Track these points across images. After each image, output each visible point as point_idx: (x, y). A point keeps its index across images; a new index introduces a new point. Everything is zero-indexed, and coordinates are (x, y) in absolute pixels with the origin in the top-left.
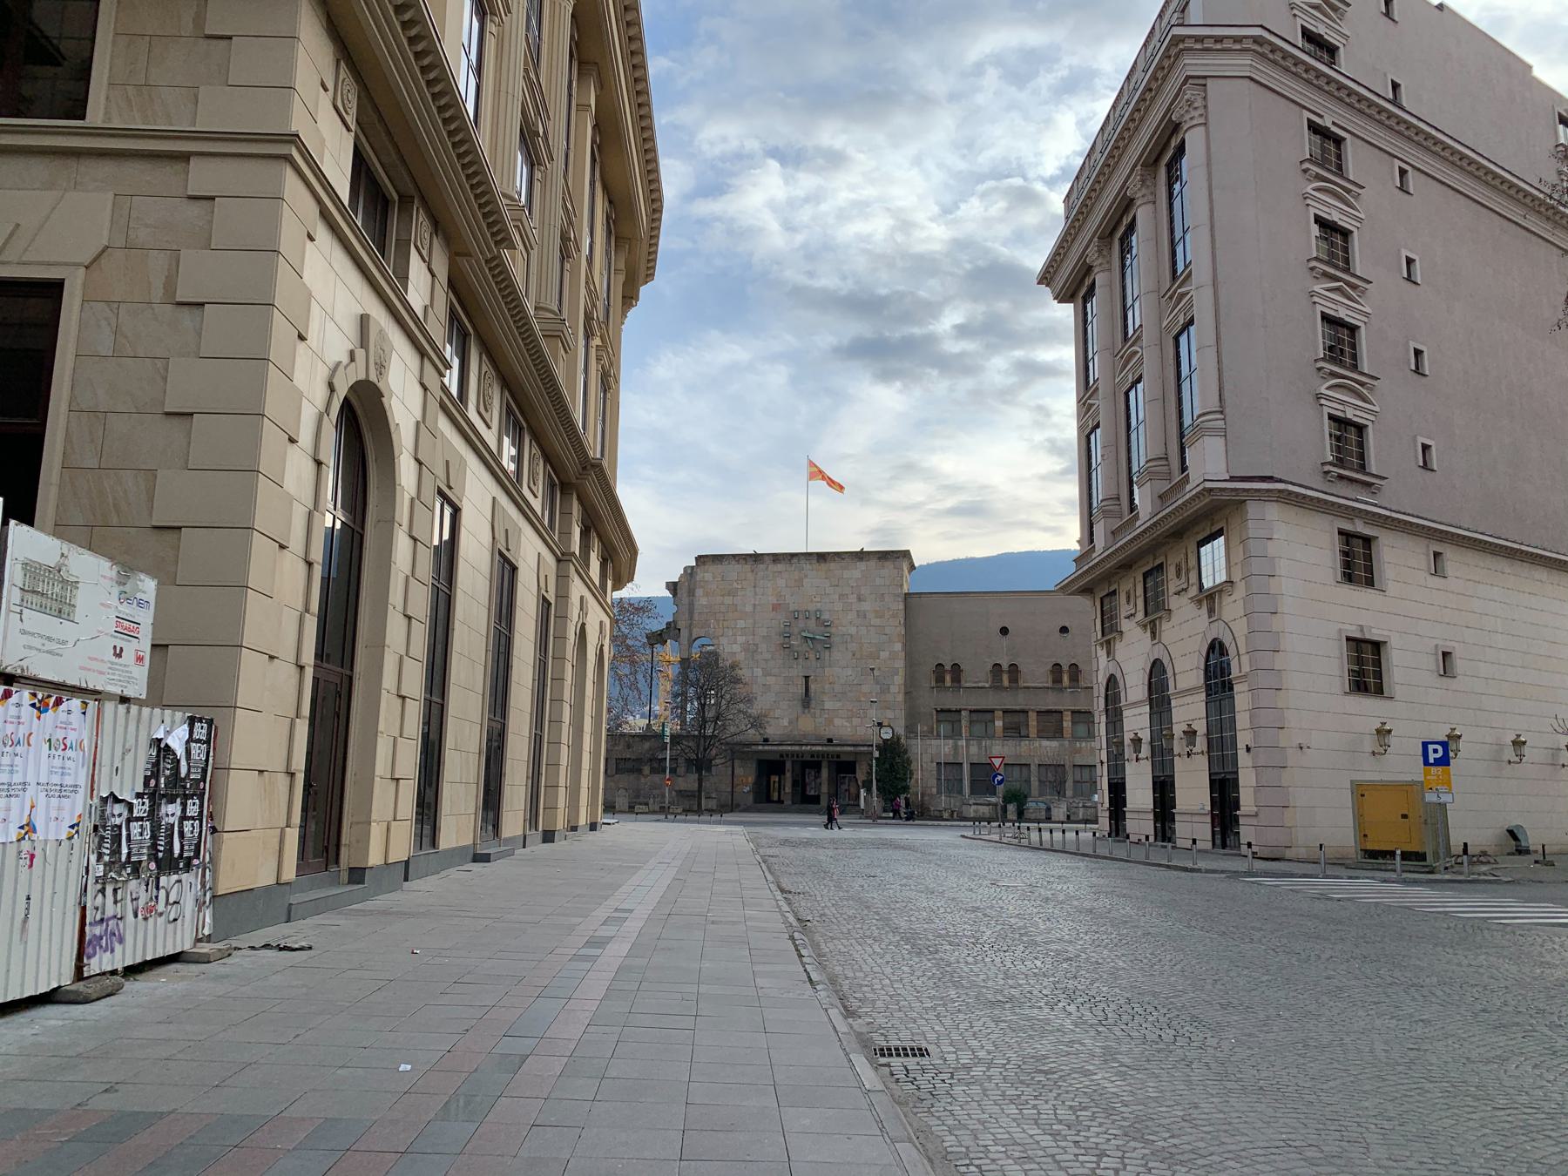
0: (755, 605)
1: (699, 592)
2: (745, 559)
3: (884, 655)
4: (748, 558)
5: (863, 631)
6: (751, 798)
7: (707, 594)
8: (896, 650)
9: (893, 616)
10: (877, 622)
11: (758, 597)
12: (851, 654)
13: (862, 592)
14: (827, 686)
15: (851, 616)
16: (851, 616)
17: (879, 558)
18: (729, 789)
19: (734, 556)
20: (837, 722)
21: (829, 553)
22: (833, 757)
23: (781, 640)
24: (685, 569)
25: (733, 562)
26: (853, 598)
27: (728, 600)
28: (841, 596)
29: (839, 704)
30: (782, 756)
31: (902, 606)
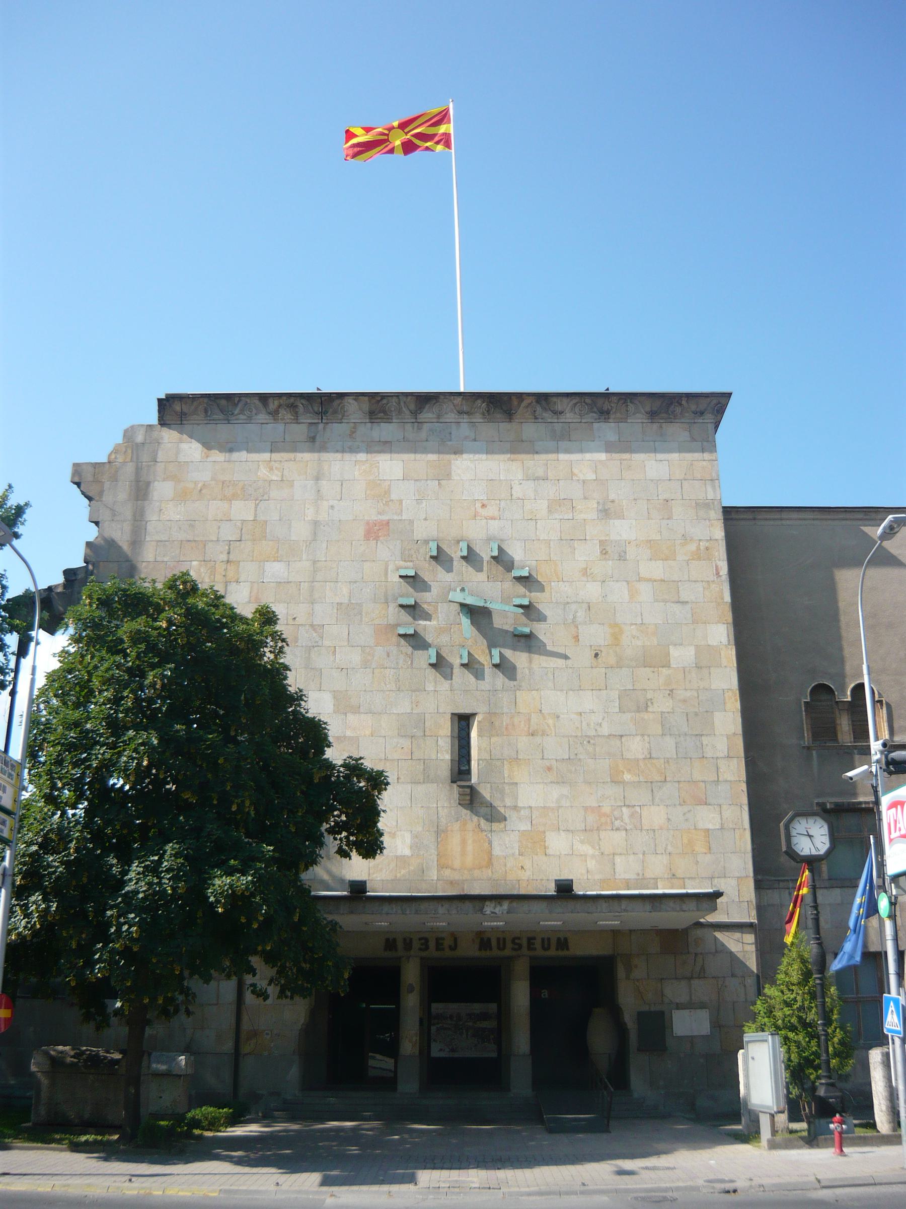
0: (316, 523)
1: (162, 490)
2: (292, 407)
3: (681, 656)
4: (299, 403)
5: (619, 592)
6: (294, 1073)
7: (182, 496)
8: (713, 642)
9: (697, 556)
10: (656, 570)
11: (325, 504)
12: (588, 654)
13: (612, 496)
14: (523, 742)
15: (586, 553)
16: (586, 553)
17: (653, 415)
18: (228, 1046)
19: (264, 398)
20: (557, 843)
21: (520, 396)
22: (546, 944)
23: (393, 613)
24: (129, 434)
25: (262, 417)
26: (588, 511)
27: (242, 510)
28: (555, 505)
29: (555, 792)
30: (390, 944)
31: (719, 533)
